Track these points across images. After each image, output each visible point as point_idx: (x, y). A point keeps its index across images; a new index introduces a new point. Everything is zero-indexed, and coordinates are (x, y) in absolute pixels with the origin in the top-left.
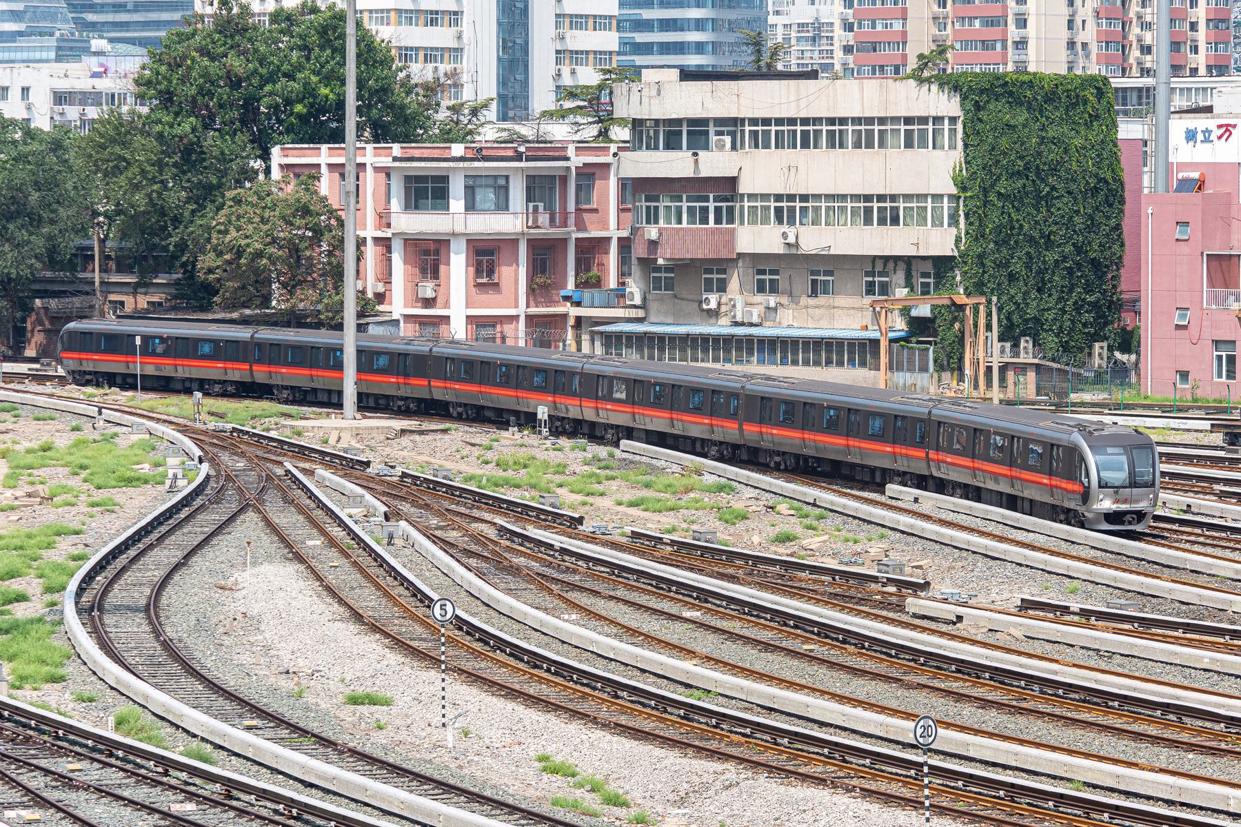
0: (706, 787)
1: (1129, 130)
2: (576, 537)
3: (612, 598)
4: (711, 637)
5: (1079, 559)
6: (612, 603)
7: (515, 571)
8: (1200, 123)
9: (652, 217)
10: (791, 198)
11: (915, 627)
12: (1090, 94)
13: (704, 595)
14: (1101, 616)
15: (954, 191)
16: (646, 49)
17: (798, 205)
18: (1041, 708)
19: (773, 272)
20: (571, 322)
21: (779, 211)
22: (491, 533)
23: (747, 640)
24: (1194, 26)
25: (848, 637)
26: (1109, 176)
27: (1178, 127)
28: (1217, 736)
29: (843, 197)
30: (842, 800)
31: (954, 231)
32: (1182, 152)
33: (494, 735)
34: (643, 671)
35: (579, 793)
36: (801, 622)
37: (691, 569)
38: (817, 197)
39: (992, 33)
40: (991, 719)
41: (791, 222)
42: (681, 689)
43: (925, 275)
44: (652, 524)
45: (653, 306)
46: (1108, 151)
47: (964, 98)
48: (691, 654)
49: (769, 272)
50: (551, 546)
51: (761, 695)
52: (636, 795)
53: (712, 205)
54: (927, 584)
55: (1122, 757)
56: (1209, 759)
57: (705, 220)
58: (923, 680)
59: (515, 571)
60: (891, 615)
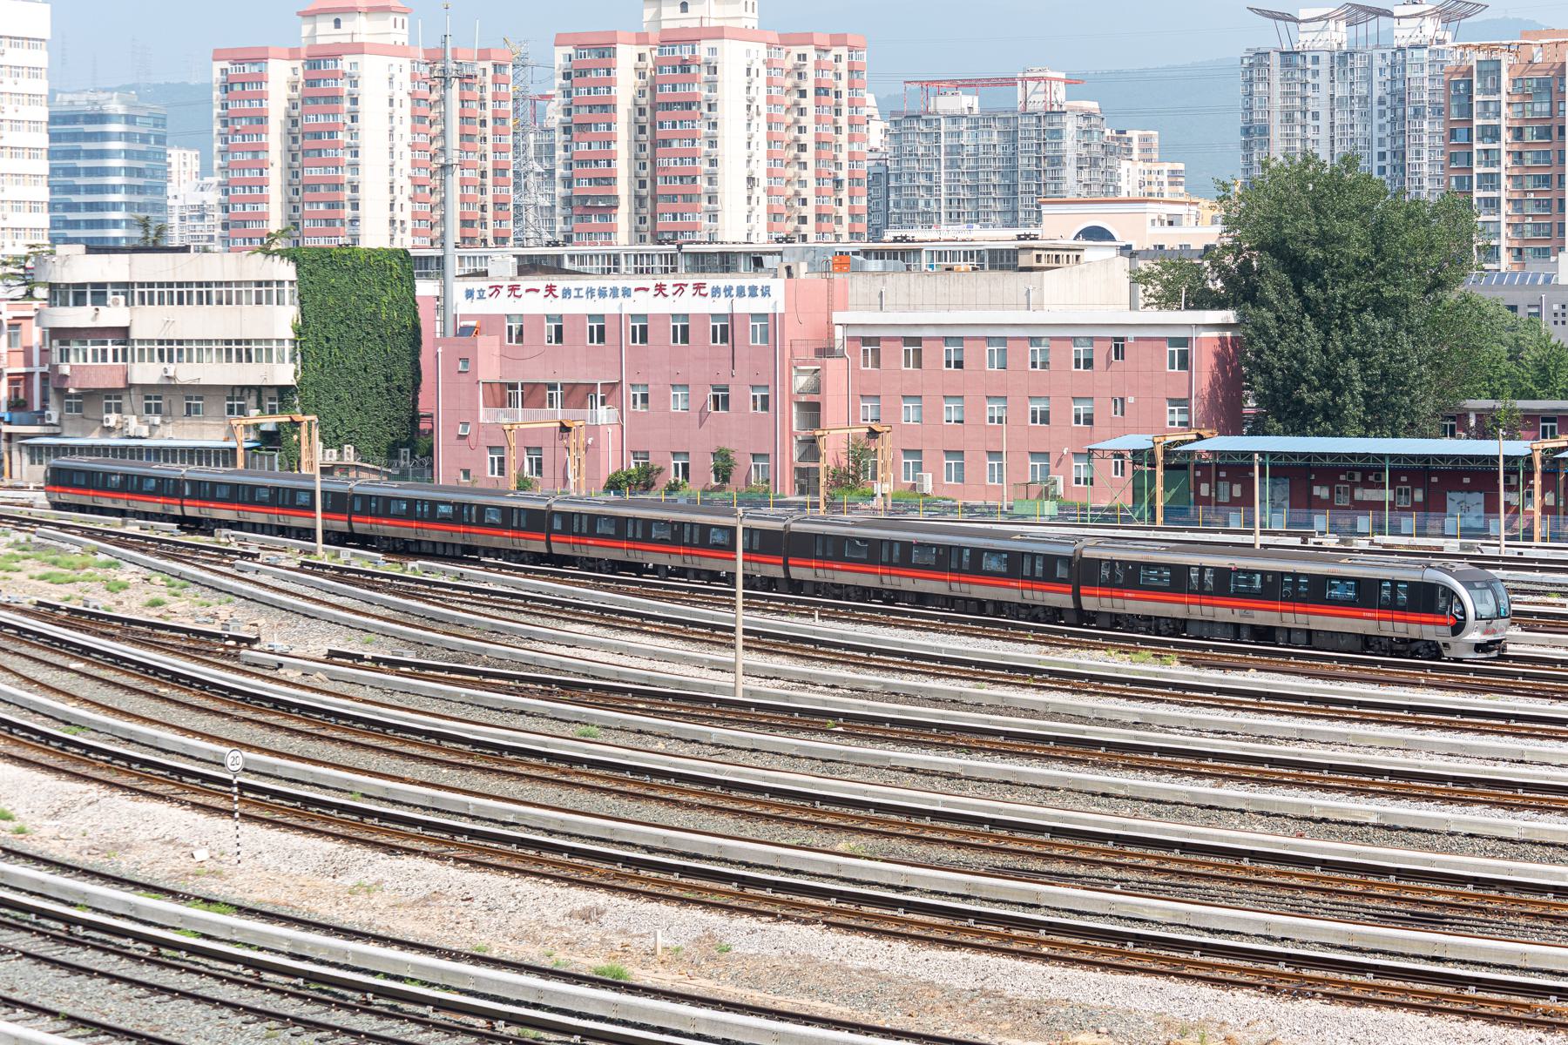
1: (425, 288)
3: (16, 654)
4: (90, 684)
5: (374, 616)
6: (17, 658)
9: (64, 356)
10: (170, 342)
11: (244, 672)
13: (87, 650)
14: (387, 662)
15: (292, 336)
17: (175, 347)
18: (335, 734)
21: (161, 352)
23: (116, 685)
24: (483, 208)
25: (192, 682)
26: (409, 323)
29: (209, 342)
31: (293, 366)
34: (34, 712)
36: (157, 670)
37: (81, 630)
38: (190, 341)
39: (331, 214)
40: (298, 745)
41: (171, 360)
42: (62, 726)
43: (271, 399)
44: (54, 595)
54: (258, 640)
55: (393, 773)
56: (458, 773)
57: (104, 359)
58: (249, 714)
60: (229, 663)
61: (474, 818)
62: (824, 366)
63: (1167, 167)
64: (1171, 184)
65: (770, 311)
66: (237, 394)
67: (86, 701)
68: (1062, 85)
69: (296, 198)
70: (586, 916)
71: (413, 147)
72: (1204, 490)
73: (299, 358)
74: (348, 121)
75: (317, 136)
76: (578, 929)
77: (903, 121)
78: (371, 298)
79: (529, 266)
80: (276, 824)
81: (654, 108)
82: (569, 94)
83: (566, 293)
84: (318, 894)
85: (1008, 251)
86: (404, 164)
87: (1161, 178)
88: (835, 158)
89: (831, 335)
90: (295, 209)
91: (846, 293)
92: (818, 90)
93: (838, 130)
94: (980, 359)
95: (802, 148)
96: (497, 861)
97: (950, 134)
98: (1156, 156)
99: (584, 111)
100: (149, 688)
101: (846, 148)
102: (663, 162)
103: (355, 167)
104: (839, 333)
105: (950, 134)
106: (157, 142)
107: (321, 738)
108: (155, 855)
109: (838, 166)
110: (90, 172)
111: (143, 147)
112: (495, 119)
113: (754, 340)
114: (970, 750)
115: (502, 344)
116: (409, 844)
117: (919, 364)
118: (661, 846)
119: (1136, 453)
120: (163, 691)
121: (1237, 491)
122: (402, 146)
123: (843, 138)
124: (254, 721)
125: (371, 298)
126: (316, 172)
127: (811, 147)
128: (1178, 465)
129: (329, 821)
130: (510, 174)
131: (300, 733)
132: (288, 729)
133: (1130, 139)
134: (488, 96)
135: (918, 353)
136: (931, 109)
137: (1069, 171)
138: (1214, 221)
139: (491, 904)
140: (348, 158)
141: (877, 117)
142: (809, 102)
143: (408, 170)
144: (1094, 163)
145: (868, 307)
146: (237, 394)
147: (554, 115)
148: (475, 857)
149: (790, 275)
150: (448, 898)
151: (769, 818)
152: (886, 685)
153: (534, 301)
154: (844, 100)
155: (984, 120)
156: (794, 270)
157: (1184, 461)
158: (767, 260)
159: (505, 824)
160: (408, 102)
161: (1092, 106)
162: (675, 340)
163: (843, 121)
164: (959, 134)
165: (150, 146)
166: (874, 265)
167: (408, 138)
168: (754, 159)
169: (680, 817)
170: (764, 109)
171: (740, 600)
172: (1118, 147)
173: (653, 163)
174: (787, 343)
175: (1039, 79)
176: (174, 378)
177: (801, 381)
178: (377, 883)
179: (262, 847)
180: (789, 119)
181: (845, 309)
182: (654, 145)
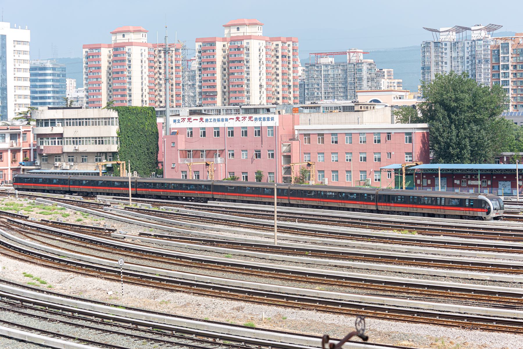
0: (66, 278)
1: (160, 120)
2: (28, 221)
7: (13, 229)
8: (177, 118)
9: (42, 143)
10: (76, 138)
12: (150, 111)
15: (117, 136)
16: (36, 104)
17: (78, 140)
19: (72, 156)
20: (21, 170)
21: (73, 141)
22: (6, 221)
27: (171, 119)
28: (191, 263)
29: (89, 138)
30: (100, 280)
32: (172, 125)
33: (11, 268)
35: (34, 281)
38: (83, 138)
40: (135, 260)
41: (77, 144)
45: (42, 165)
46: (154, 125)
47: (118, 113)
48: (59, 248)
49: (71, 157)
50: (21, 224)
51: (78, 257)
52: (48, 281)
53: (57, 140)
56: (189, 268)
57: (55, 144)
58: (117, 252)
59: (13, 229)
61: (197, 281)
62: (292, 143)
63: (396, 81)
64: (398, 86)
65: (274, 125)
66: (99, 155)
67: (63, 249)
68: (362, 54)
69: (111, 94)
70: (238, 309)
71: (149, 76)
72: (418, 182)
73: (119, 143)
74: (128, 68)
75: (118, 73)
76: (235, 313)
77: (310, 66)
78: (142, 123)
79: (192, 113)
80: (133, 283)
81: (228, 62)
82: (201, 58)
83: (207, 120)
84: (150, 304)
85: (349, 106)
86: (146, 82)
87: (394, 85)
88: (288, 78)
89: (294, 133)
90: (110, 97)
91: (299, 119)
92: (283, 56)
93: (289, 69)
94: (343, 140)
95: (278, 75)
96: (206, 293)
97: (325, 71)
98: (392, 77)
99: (205, 64)
100: (83, 244)
101: (292, 75)
102: (231, 80)
103: (130, 83)
104: (296, 132)
105: (325, 71)
106: (63, 76)
107: (142, 258)
108: (95, 293)
109: (289, 81)
110: (41, 86)
111: (58, 78)
112: (176, 67)
113: (269, 135)
114: (353, 260)
115: (185, 136)
116: (177, 289)
117: (323, 142)
118: (259, 288)
119: (396, 170)
120: (88, 245)
121: (429, 182)
122: (145, 76)
123: (291, 72)
124: (119, 254)
125: (142, 123)
126: (117, 85)
127: (280, 75)
128: (410, 173)
129: (150, 282)
130: (181, 85)
131: (135, 257)
132: (131, 256)
133: (384, 72)
134: (174, 59)
135: (323, 139)
136: (319, 62)
137: (365, 83)
138: (414, 97)
139: (207, 306)
140: (128, 80)
141: (300, 65)
142: (279, 60)
143: (147, 84)
144: (373, 79)
145: (306, 124)
146: (99, 155)
147: (195, 65)
148: (199, 292)
149: (279, 113)
150: (192, 305)
151: (292, 280)
152: (323, 241)
153: (196, 123)
154: (291, 59)
155: (336, 66)
156: (281, 112)
157: (412, 172)
158: (271, 110)
159: (207, 283)
160: (147, 62)
161: (371, 61)
162: (243, 136)
163: (291, 66)
164: (328, 71)
165: (61, 76)
166: (306, 111)
167: (147, 73)
168: (262, 79)
169: (264, 280)
170: (265, 62)
171: (276, 217)
172: (380, 74)
173: (228, 80)
174: (280, 136)
175: (354, 52)
176: (78, 150)
177: (284, 148)
178: (169, 301)
179: (130, 290)
180: (273, 65)
181: (298, 125)
182: (229, 75)
